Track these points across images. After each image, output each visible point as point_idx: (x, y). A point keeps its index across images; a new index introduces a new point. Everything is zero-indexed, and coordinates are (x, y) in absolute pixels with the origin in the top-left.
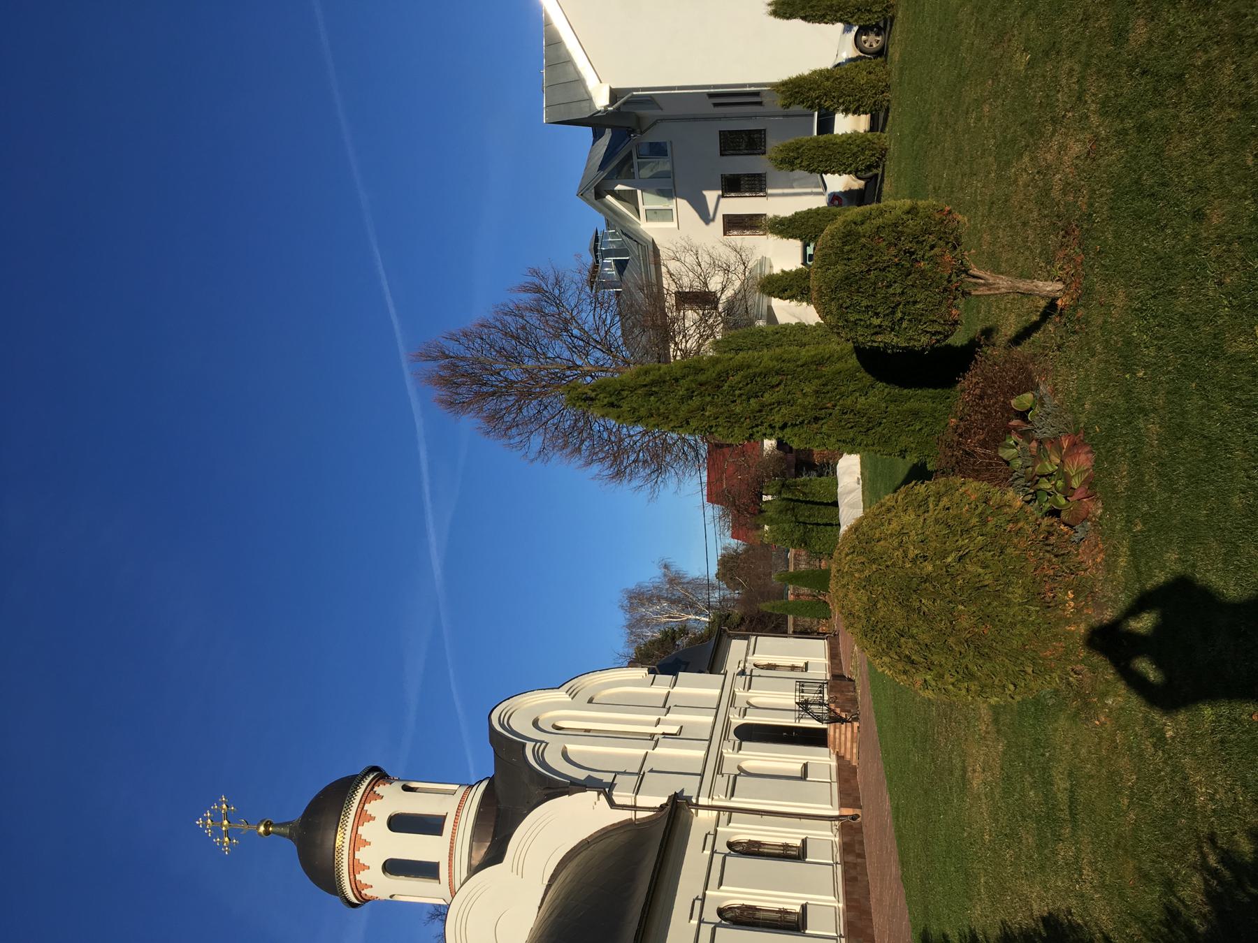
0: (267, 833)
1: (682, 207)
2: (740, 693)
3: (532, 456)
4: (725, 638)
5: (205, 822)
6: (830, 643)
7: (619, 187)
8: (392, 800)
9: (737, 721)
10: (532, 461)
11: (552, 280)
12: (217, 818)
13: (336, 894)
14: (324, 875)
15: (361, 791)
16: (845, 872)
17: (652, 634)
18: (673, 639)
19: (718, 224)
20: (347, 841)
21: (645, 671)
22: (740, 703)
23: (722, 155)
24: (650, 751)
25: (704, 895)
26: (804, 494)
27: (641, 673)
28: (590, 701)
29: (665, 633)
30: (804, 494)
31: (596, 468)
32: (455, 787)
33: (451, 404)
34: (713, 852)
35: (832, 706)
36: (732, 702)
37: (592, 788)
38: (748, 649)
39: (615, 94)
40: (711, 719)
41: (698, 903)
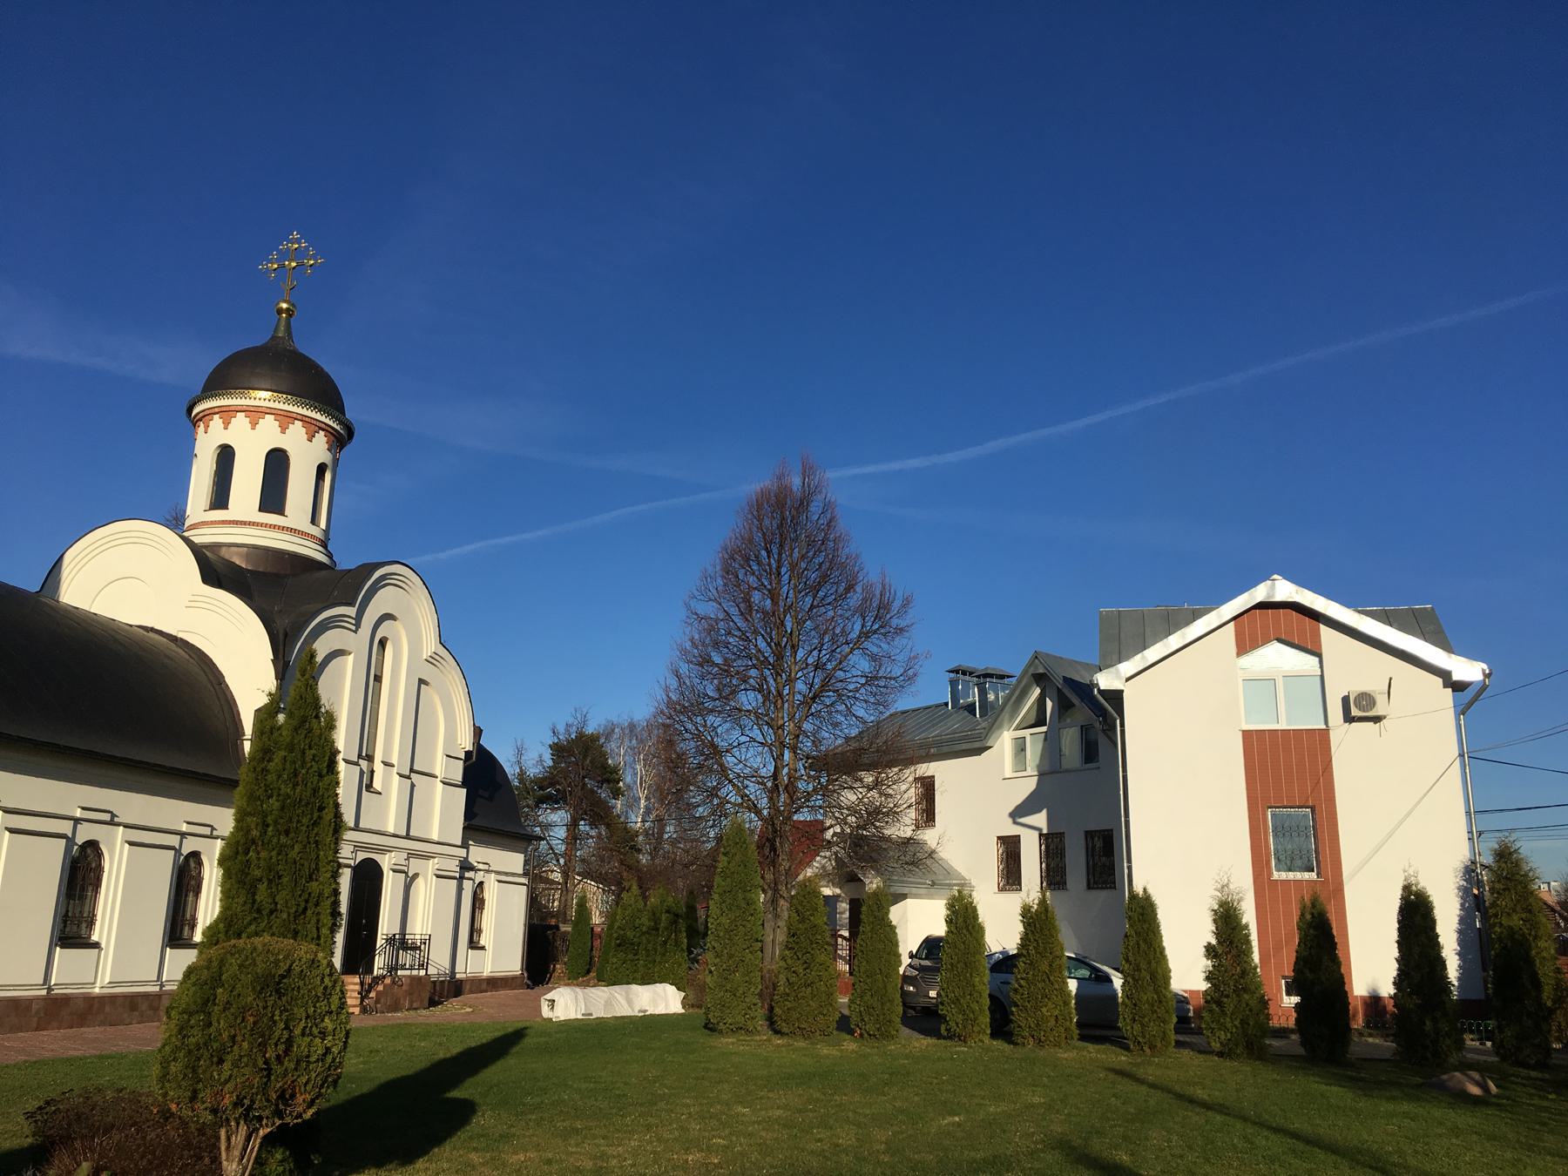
0: (280, 311)
1: (1028, 785)
2: (432, 865)
3: (693, 603)
4: (524, 844)
5: (295, 241)
6: (514, 978)
7: (1049, 704)
8: (307, 452)
9: (386, 862)
10: (687, 605)
11: (902, 624)
12: (298, 254)
13: (204, 391)
14: (224, 379)
15: (318, 416)
16: (146, 995)
17: (618, 753)
18: (608, 781)
19: (1011, 830)
20: (257, 403)
21: (469, 747)
22: (415, 866)
23: (1087, 833)
24: (340, 757)
25: (119, 824)
26: (665, 943)
27: (466, 742)
28: (421, 681)
29: (615, 770)
30: (665, 943)
31: (674, 683)
32: (323, 525)
33: (759, 507)
34: (183, 835)
35: (388, 981)
36: (412, 855)
37: (279, 687)
38: (506, 874)
39: (1116, 697)
40: (391, 830)
41: (107, 817)
